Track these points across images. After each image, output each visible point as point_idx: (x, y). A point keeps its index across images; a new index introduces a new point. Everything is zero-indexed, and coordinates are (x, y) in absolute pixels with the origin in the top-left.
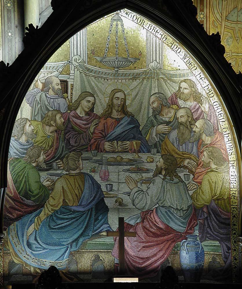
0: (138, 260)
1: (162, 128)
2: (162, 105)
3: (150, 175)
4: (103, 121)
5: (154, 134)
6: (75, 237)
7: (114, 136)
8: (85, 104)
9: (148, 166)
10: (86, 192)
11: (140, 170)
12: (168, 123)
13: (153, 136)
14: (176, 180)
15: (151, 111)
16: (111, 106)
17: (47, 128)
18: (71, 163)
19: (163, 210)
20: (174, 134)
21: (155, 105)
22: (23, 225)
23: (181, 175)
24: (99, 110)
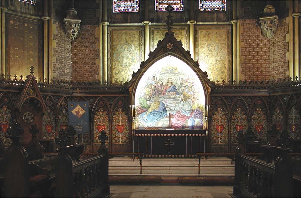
0: (175, 124)
1: (183, 88)
2: (183, 82)
3: (179, 101)
4: (165, 87)
5: (181, 90)
6: (157, 118)
7: (169, 91)
8: (160, 83)
9: (179, 99)
10: (160, 106)
11: (176, 100)
12: (185, 87)
13: (180, 90)
14: (187, 102)
15: (180, 84)
16: (168, 83)
17: (149, 89)
18: (156, 99)
19: (183, 111)
20: (187, 90)
21: (181, 82)
22: (142, 115)
23: (189, 101)
24: (164, 84)
